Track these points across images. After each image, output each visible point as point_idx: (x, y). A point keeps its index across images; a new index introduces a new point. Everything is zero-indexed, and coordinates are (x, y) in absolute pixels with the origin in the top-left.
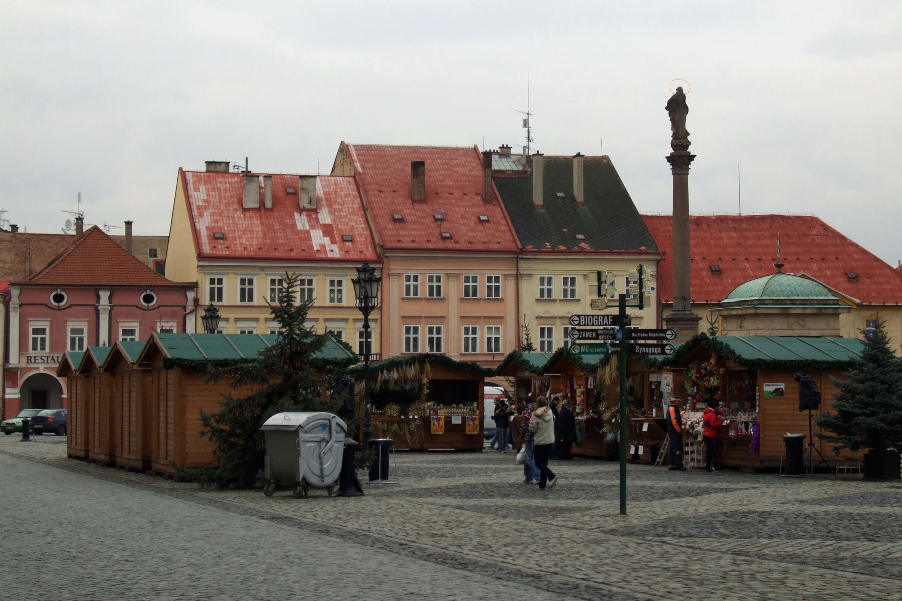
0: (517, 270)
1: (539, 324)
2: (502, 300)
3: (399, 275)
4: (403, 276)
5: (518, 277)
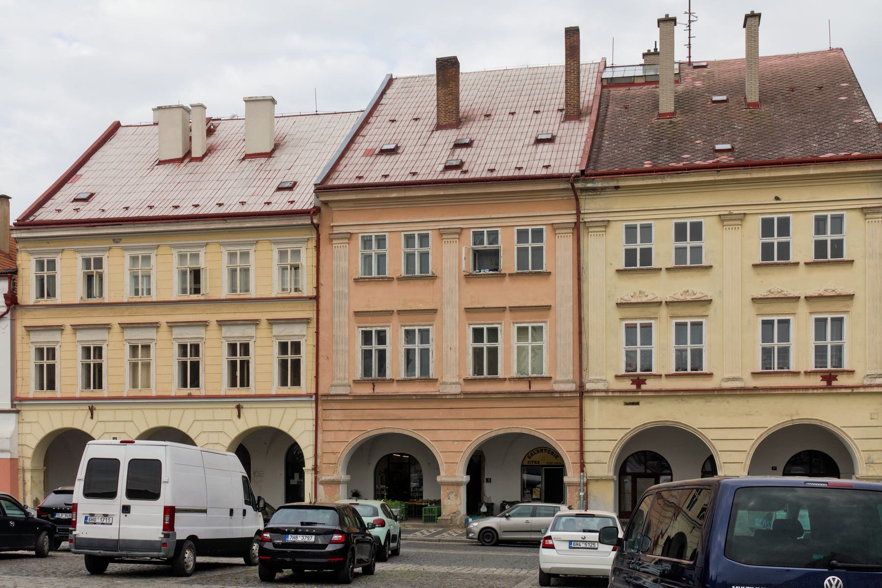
0: (578, 213)
1: (622, 319)
2: (549, 274)
3: (350, 236)
4: (357, 239)
5: (578, 228)
